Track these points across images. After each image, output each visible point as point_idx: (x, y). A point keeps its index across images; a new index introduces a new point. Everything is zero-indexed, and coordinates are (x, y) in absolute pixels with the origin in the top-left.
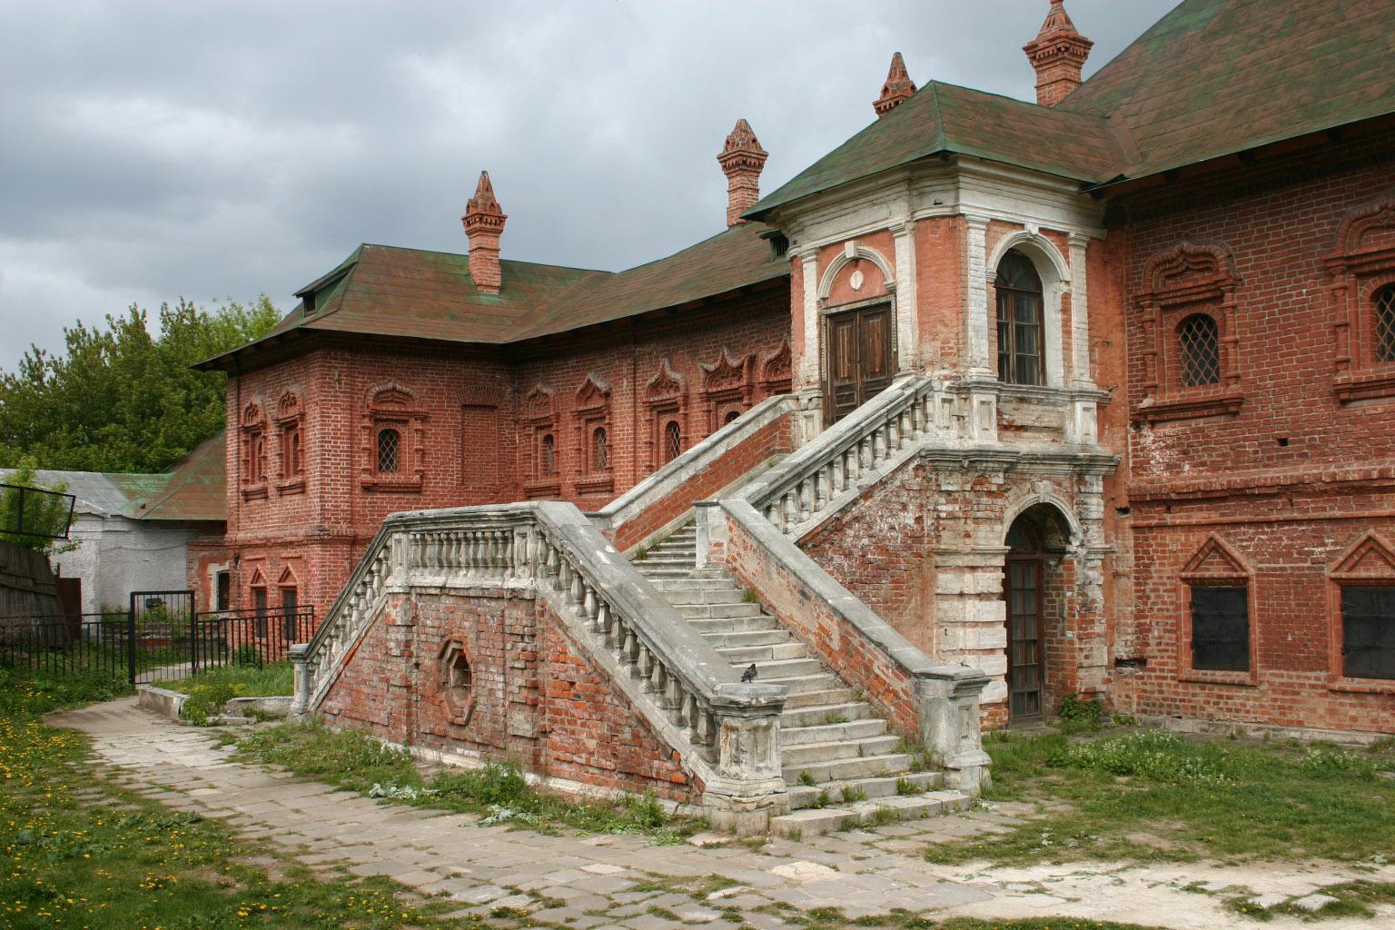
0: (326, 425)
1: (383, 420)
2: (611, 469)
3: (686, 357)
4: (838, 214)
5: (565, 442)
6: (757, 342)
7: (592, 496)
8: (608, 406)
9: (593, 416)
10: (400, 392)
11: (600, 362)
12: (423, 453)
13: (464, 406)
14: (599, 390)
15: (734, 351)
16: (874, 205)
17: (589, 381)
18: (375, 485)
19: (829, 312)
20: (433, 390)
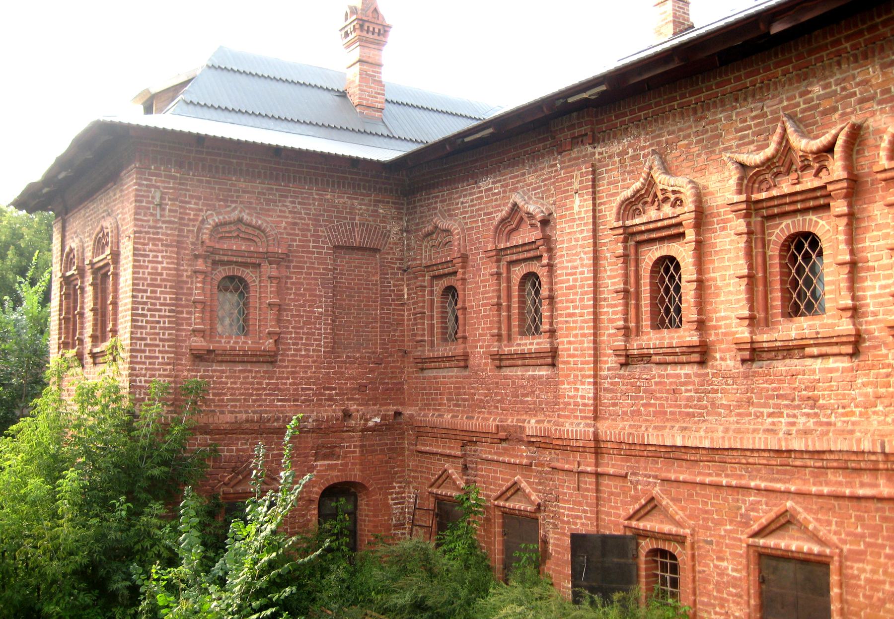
0: (141, 267)
1: (223, 263)
2: (552, 332)
3: (695, 149)
5: (475, 294)
6: (862, 101)
7: (519, 372)
8: (547, 240)
9: (521, 256)
10: (248, 225)
11: (531, 178)
12: (280, 308)
13: (336, 248)
14: (531, 216)
15: (805, 127)
17: (515, 204)
18: (210, 352)
20: (295, 224)
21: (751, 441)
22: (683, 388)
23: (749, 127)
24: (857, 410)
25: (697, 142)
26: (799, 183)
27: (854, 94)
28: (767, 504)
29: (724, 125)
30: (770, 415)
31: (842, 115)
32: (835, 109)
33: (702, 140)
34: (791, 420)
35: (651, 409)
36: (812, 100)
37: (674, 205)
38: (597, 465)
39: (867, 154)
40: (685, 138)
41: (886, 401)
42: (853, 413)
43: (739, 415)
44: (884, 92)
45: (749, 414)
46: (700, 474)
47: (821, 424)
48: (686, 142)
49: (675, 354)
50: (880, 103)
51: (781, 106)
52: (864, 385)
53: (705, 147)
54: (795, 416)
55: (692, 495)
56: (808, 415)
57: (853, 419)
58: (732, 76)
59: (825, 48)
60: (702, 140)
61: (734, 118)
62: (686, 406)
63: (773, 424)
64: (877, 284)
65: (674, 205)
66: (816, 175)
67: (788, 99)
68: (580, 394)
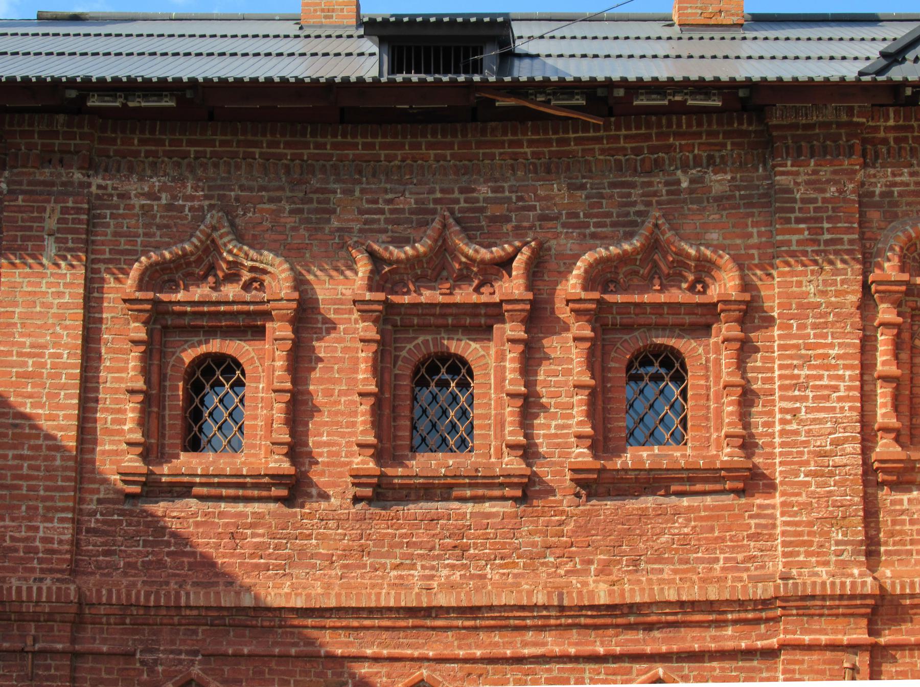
3: (290, 221)
6: (543, 218)
21: (373, 597)
22: (249, 532)
23: (382, 212)
24: (521, 561)
25: (292, 212)
26: (451, 294)
27: (534, 208)
28: (388, 676)
29: (340, 199)
30: (396, 567)
31: (517, 228)
32: (508, 220)
33: (300, 211)
34: (427, 572)
35: (186, 560)
36: (477, 200)
37: (247, 287)
38: (73, 641)
39: (546, 278)
40: (271, 200)
41: (558, 552)
42: (515, 565)
43: (344, 566)
44: (571, 215)
45: (364, 566)
46: (276, 644)
47: (472, 577)
48: (273, 206)
49: (243, 486)
50: (564, 225)
51: (432, 197)
52: (530, 533)
53: (308, 221)
54: (433, 568)
55: (262, 673)
56: (453, 567)
57: (516, 571)
58: (360, 140)
59: (501, 144)
60: (300, 211)
61: (357, 194)
62: (252, 556)
63: (401, 577)
64: (554, 423)
65: (247, 287)
66: (477, 290)
67: (442, 191)
68: (41, 534)
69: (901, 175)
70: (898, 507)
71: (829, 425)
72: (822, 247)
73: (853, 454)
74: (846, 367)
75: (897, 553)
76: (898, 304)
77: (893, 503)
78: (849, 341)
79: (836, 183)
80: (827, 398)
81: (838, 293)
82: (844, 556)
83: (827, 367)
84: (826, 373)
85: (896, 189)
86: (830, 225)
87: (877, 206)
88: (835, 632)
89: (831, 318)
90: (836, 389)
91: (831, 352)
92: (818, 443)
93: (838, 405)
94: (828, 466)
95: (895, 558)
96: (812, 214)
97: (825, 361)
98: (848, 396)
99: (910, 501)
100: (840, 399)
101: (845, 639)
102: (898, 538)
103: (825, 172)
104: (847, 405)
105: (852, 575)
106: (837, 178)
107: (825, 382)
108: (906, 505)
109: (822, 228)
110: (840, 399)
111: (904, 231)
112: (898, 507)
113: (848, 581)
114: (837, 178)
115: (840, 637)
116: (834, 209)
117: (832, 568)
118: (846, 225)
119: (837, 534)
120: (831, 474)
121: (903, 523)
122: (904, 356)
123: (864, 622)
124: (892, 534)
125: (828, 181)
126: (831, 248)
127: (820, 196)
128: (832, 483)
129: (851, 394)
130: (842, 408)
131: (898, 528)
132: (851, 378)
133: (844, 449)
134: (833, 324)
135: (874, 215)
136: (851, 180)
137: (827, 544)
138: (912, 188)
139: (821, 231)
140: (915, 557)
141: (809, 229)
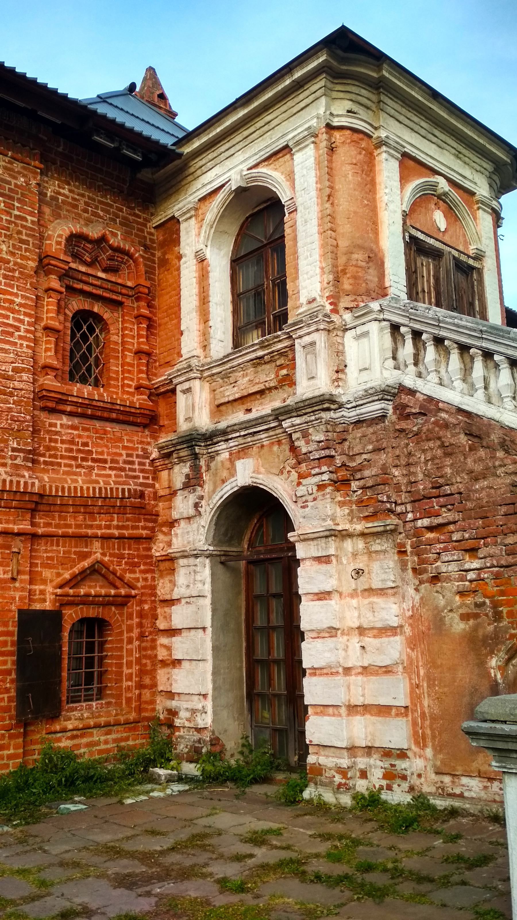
4: (423, 132)
16: (458, 157)
19: (414, 232)
69: (64, 189)
70: (53, 429)
71: (12, 355)
72: (13, 219)
73: (27, 382)
74: (25, 314)
75: (52, 464)
76: (61, 278)
77: (51, 425)
78: (28, 295)
79: (24, 176)
80: (12, 334)
81: (22, 257)
82: (18, 461)
83: (13, 311)
84: (12, 315)
85: (60, 197)
86: (19, 205)
87: (49, 204)
88: (8, 522)
89: (17, 274)
90: (18, 329)
91: (16, 299)
92: (3, 368)
93: (19, 342)
94: (9, 388)
95: (50, 467)
96: (7, 192)
97: (12, 306)
98: (26, 337)
99: (62, 425)
100: (20, 337)
101: (16, 528)
102: (53, 452)
103: (17, 166)
104: (25, 343)
105: (24, 476)
106: (26, 173)
107: (11, 322)
108: (58, 429)
109: (14, 205)
110: (20, 337)
111: (69, 228)
112: (53, 429)
113: (22, 481)
114: (26, 173)
115: (11, 526)
116: (23, 195)
117: (8, 469)
118: (30, 209)
119: (13, 442)
120: (11, 395)
121: (56, 441)
122: (61, 318)
123: (28, 516)
124: (48, 448)
125: (19, 173)
126: (19, 222)
127: (13, 181)
128: (12, 402)
129: (28, 336)
130: (21, 345)
131: (53, 444)
132: (29, 324)
133: (21, 377)
134: (19, 279)
135: (47, 210)
136: (35, 178)
137: (6, 450)
138: (70, 200)
139: (12, 207)
140: (63, 468)
141: (4, 202)
